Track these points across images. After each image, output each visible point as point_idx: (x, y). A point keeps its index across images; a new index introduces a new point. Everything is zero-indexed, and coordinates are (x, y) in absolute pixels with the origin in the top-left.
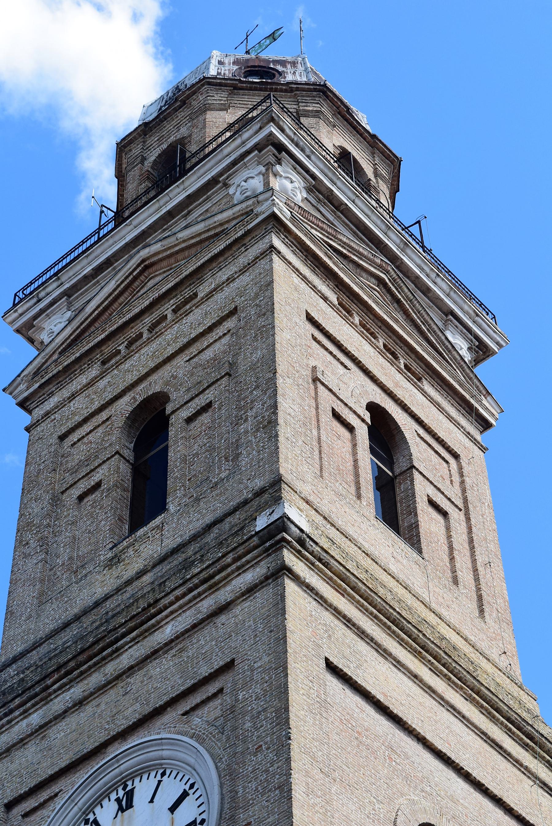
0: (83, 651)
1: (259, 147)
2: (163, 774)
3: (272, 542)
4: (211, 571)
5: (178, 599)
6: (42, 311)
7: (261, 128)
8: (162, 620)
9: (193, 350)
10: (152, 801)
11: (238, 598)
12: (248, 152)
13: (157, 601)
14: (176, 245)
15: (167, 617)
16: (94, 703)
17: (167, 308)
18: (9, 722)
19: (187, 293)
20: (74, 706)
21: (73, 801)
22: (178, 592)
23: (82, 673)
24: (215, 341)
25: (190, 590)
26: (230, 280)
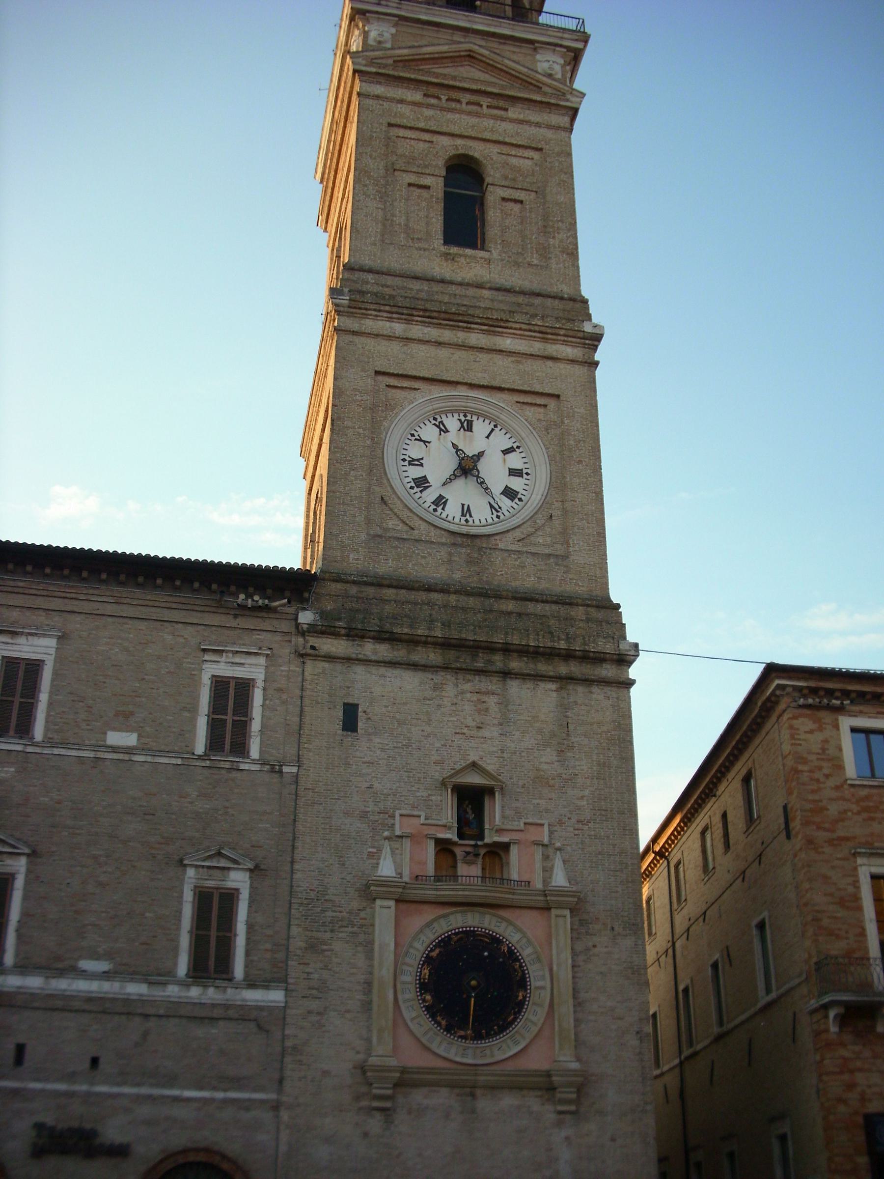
0: (445, 312)
1: (569, 49)
2: (496, 426)
3: (590, 342)
4: (549, 331)
5: (520, 329)
6: (377, 13)
7: (577, 40)
8: (506, 333)
9: (505, 149)
10: (488, 437)
11: (565, 360)
12: (561, 46)
13: (507, 321)
14: (499, 63)
15: (510, 334)
16: (451, 351)
17: (485, 101)
18: (376, 316)
19: (501, 103)
20: (435, 342)
21: (431, 402)
22: (524, 327)
23: (440, 324)
24: (521, 157)
25: (530, 331)
26: (538, 125)
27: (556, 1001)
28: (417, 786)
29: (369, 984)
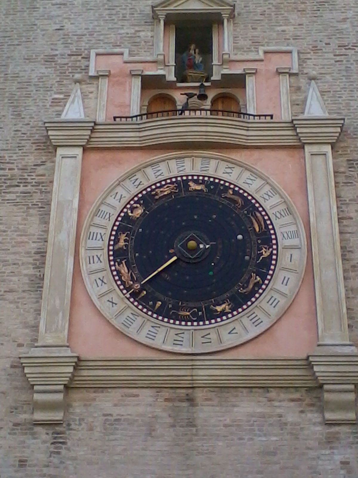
27: (316, 261)
28: (120, 23)
29: (42, 254)
